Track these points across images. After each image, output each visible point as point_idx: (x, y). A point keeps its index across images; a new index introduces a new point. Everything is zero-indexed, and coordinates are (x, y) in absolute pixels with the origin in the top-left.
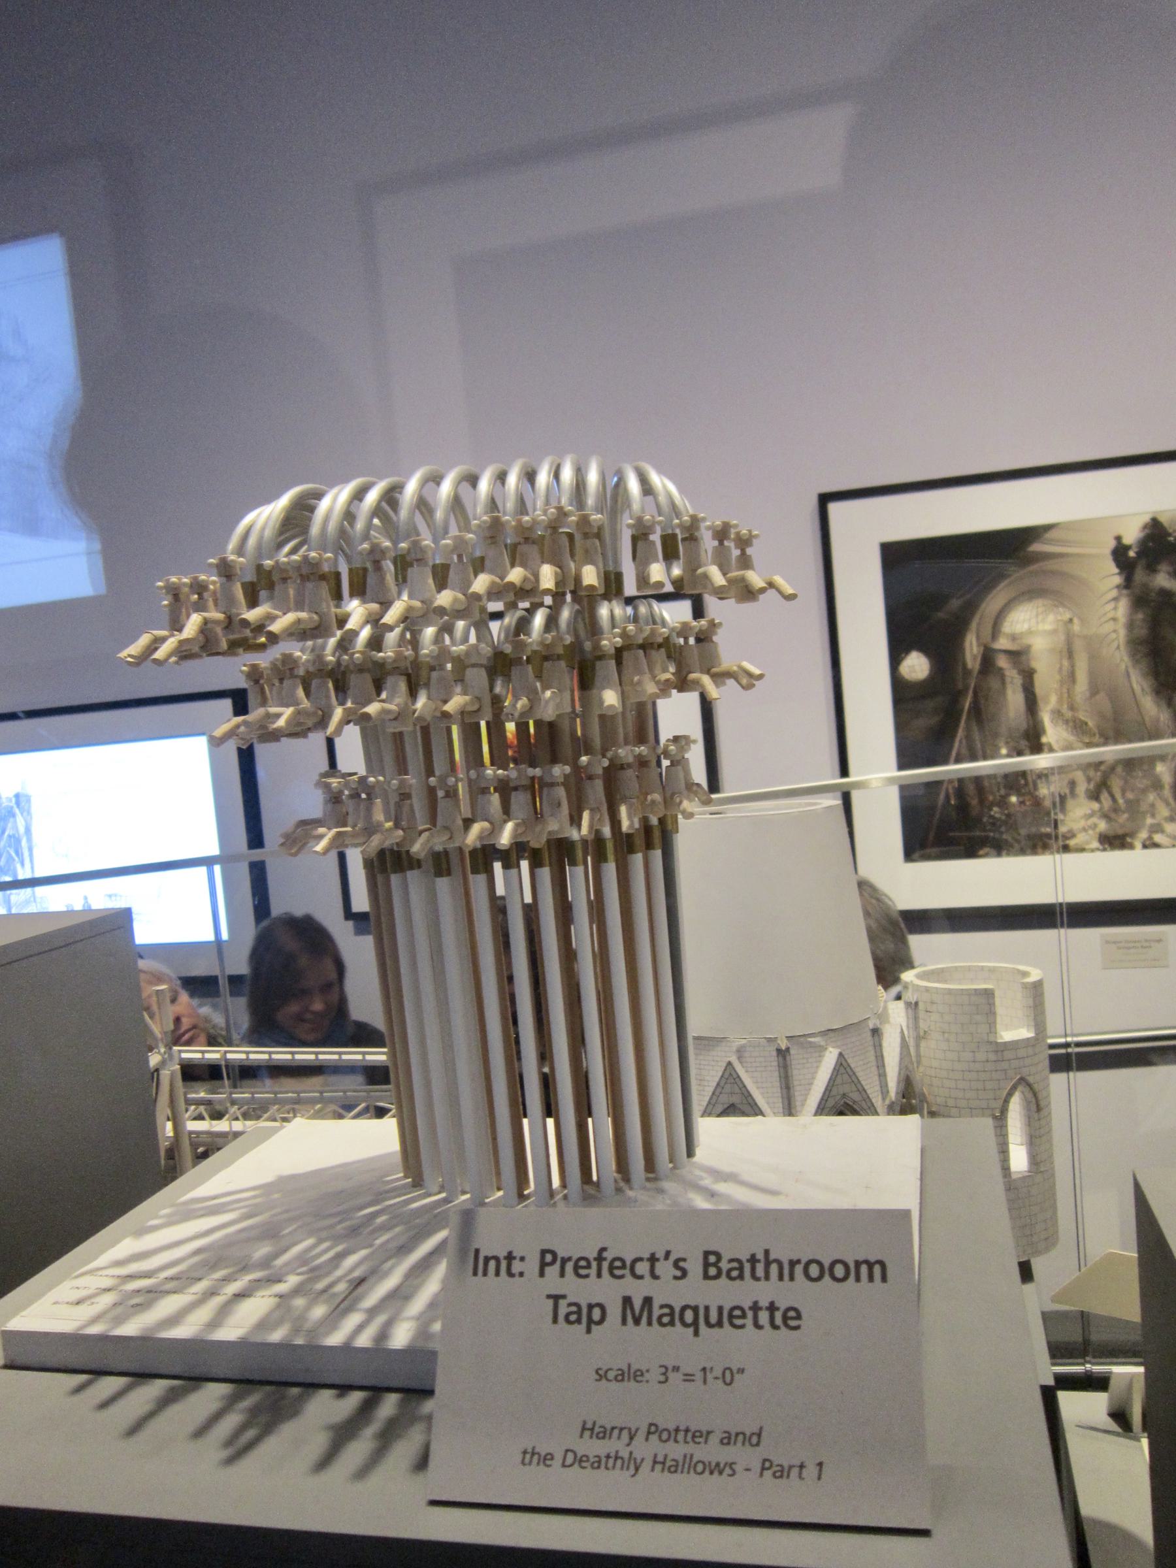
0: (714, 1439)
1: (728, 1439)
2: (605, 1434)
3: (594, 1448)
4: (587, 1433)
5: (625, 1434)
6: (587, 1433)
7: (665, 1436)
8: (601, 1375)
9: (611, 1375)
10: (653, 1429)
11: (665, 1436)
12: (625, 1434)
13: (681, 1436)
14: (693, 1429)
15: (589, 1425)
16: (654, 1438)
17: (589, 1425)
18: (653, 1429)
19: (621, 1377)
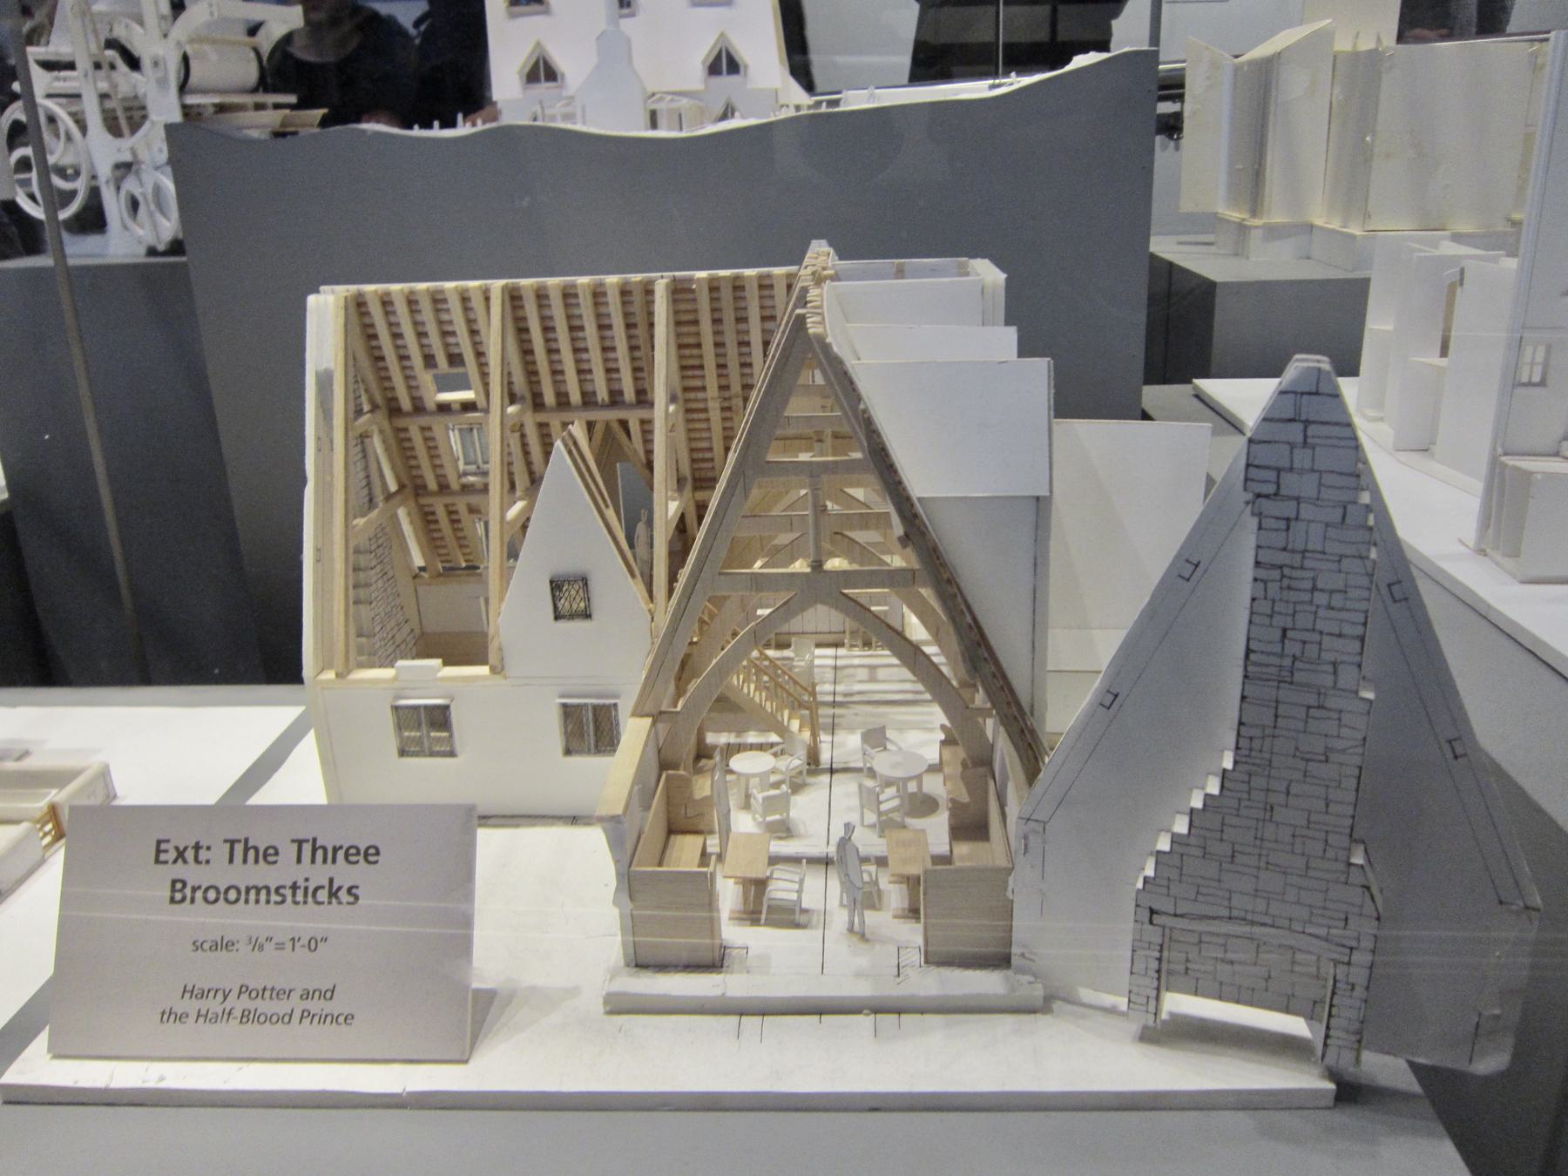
0: (295, 996)
1: (307, 995)
2: (203, 995)
3: (191, 1006)
4: (187, 995)
5: (220, 994)
6: (187, 995)
7: (254, 994)
8: (198, 946)
9: (206, 946)
10: (243, 990)
11: (254, 994)
12: (220, 994)
13: (267, 994)
14: (278, 987)
15: (189, 988)
16: (244, 997)
17: (189, 988)
18: (243, 990)
19: (215, 947)
